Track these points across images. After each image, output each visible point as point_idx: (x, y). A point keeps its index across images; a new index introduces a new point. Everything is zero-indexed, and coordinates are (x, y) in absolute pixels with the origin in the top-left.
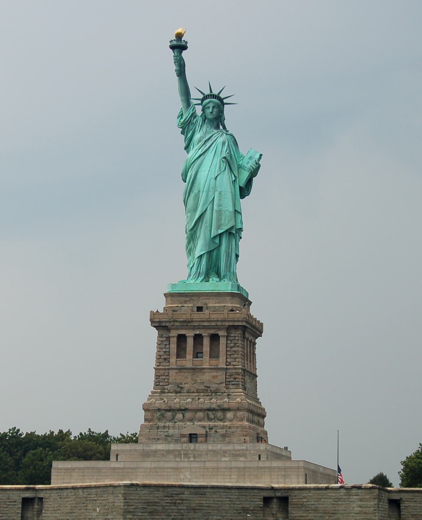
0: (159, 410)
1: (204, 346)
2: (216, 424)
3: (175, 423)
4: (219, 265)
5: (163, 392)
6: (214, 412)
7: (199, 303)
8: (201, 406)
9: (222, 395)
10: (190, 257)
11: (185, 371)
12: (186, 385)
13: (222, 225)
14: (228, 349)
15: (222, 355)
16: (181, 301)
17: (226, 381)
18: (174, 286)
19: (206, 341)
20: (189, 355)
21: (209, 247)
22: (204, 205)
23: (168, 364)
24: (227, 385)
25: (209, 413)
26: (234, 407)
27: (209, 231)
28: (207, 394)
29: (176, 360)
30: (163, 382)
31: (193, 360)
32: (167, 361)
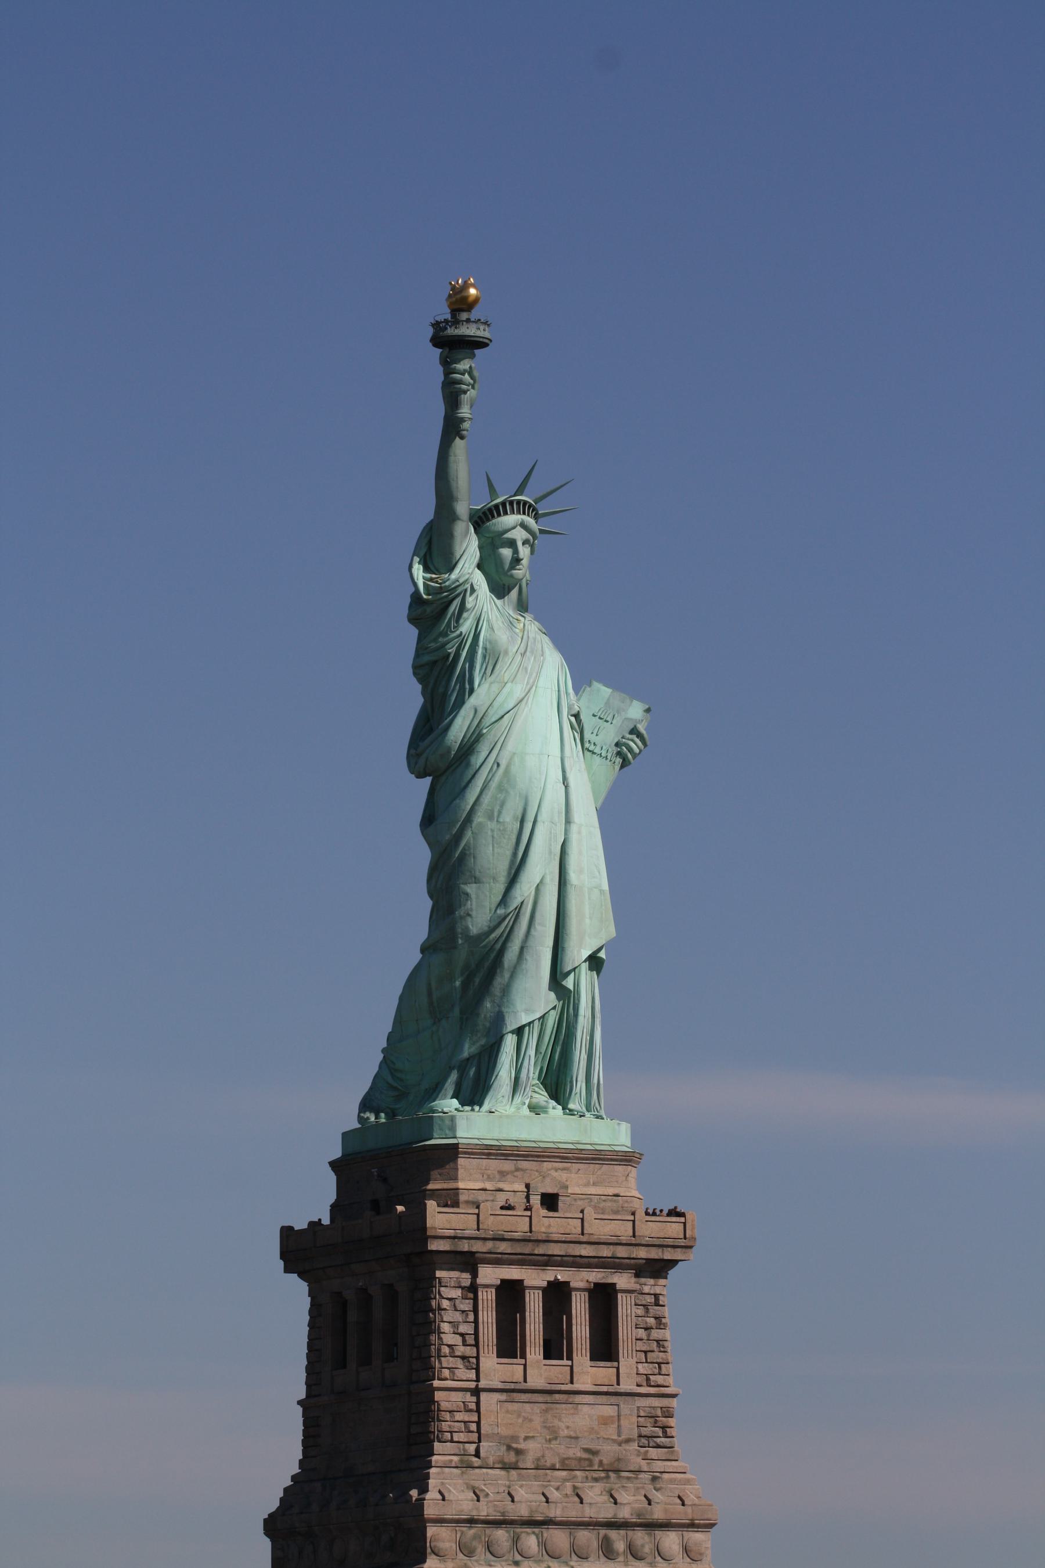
0: (471, 1521)
6: (622, 1532)
7: (548, 1180)
8: (589, 1513)
9: (637, 1478)
17: (640, 1436)
18: (465, 1121)
24: (641, 1447)
26: (679, 1518)
28: (595, 1475)
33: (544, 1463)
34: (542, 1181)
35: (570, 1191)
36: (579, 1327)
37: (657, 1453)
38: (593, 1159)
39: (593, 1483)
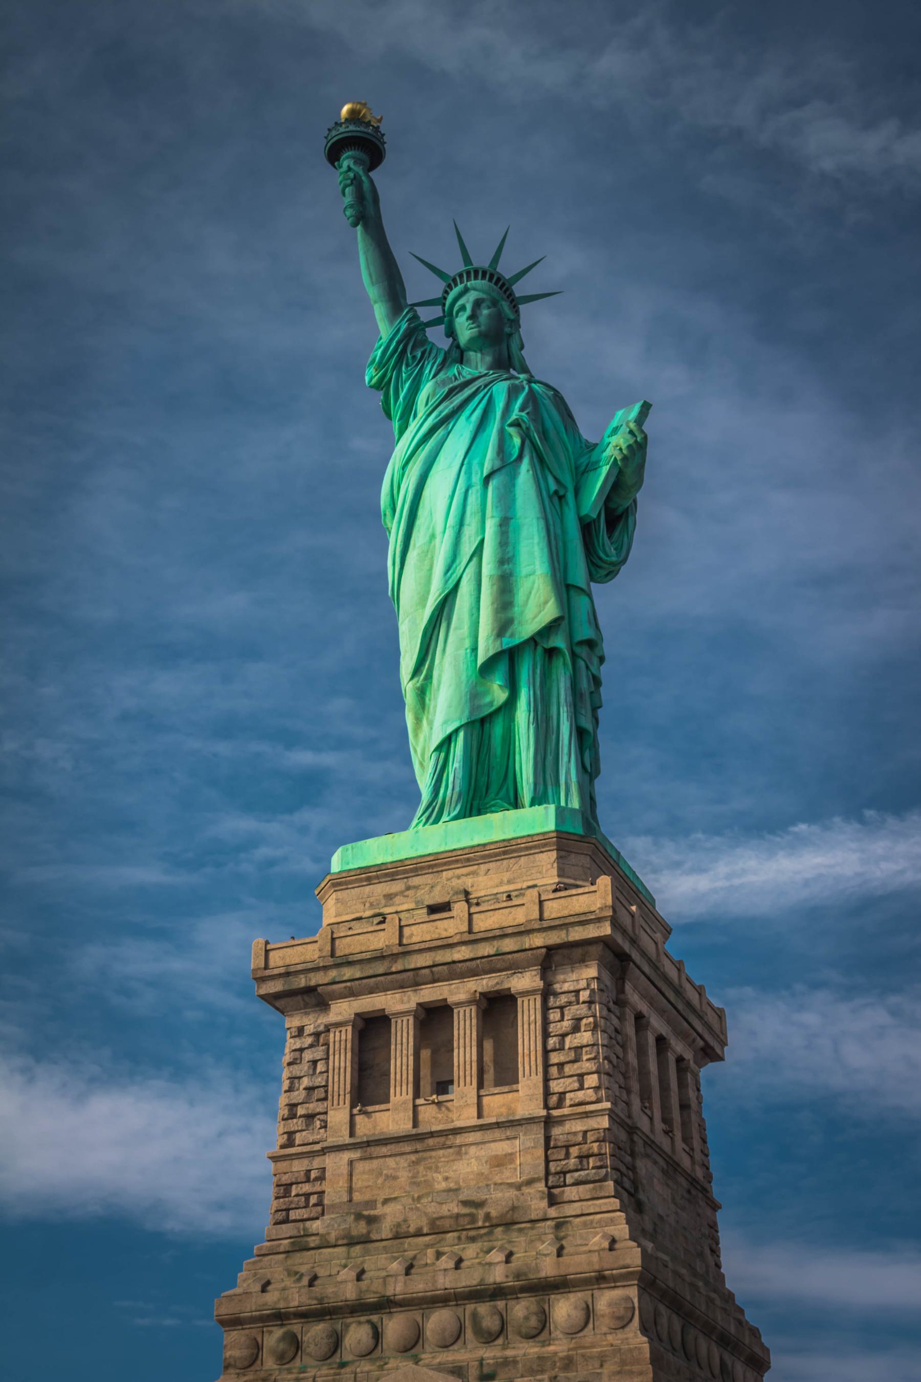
0: (280, 1317)
2: (509, 1353)
3: (343, 1365)
5: (299, 1245)
6: (501, 1304)
7: (438, 888)
9: (532, 1228)
11: (384, 1150)
12: (389, 1209)
13: (516, 622)
14: (552, 1042)
15: (527, 1068)
16: (372, 899)
17: (547, 1173)
20: (398, 1089)
21: (473, 709)
24: (554, 1187)
25: (479, 1309)
26: (579, 1270)
27: (468, 651)
29: (352, 1116)
30: (305, 1207)
31: (415, 1107)
32: (318, 1122)
33: (406, 1229)
34: (430, 892)
35: (471, 897)
36: (462, 1050)
37: (578, 1192)
38: (504, 853)
39: (468, 1244)
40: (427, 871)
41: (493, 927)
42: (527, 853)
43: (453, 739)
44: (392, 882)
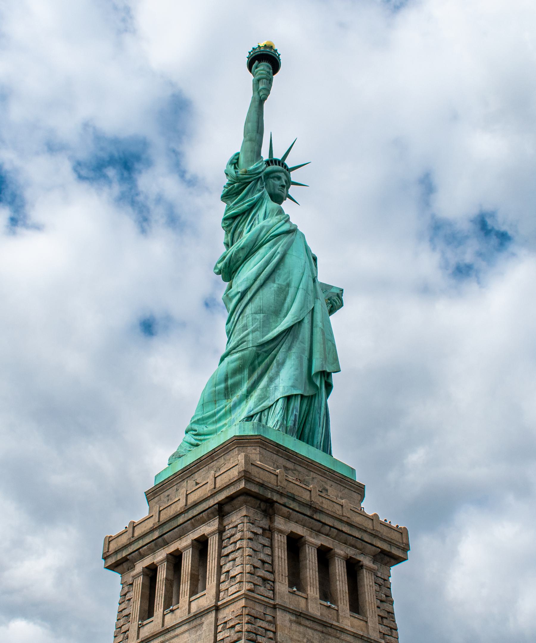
1: (338, 579)
4: (307, 431)
7: (315, 481)
10: (224, 403)
11: (308, 623)
18: (262, 427)
19: (340, 567)
21: (305, 389)
22: (302, 311)
23: (270, 594)
27: (307, 358)
30: (264, 637)
36: (341, 582)
40: (305, 466)
41: (359, 522)
42: (349, 488)
43: (294, 398)
44: (287, 461)
